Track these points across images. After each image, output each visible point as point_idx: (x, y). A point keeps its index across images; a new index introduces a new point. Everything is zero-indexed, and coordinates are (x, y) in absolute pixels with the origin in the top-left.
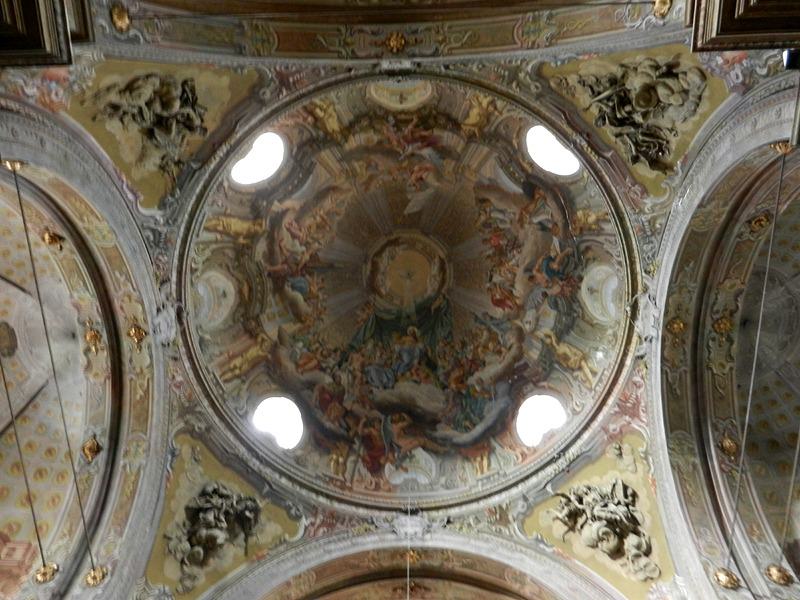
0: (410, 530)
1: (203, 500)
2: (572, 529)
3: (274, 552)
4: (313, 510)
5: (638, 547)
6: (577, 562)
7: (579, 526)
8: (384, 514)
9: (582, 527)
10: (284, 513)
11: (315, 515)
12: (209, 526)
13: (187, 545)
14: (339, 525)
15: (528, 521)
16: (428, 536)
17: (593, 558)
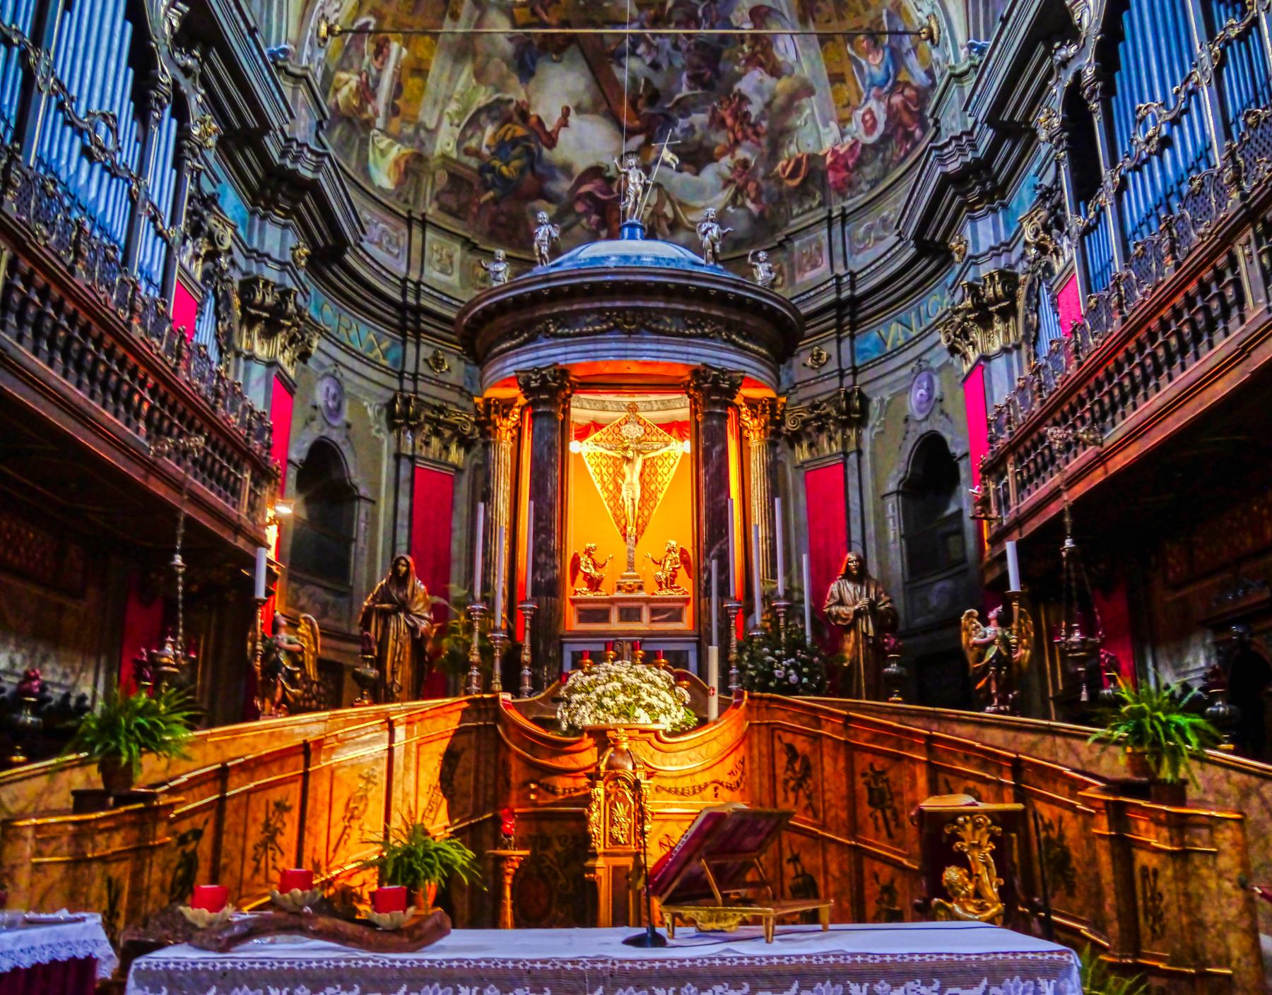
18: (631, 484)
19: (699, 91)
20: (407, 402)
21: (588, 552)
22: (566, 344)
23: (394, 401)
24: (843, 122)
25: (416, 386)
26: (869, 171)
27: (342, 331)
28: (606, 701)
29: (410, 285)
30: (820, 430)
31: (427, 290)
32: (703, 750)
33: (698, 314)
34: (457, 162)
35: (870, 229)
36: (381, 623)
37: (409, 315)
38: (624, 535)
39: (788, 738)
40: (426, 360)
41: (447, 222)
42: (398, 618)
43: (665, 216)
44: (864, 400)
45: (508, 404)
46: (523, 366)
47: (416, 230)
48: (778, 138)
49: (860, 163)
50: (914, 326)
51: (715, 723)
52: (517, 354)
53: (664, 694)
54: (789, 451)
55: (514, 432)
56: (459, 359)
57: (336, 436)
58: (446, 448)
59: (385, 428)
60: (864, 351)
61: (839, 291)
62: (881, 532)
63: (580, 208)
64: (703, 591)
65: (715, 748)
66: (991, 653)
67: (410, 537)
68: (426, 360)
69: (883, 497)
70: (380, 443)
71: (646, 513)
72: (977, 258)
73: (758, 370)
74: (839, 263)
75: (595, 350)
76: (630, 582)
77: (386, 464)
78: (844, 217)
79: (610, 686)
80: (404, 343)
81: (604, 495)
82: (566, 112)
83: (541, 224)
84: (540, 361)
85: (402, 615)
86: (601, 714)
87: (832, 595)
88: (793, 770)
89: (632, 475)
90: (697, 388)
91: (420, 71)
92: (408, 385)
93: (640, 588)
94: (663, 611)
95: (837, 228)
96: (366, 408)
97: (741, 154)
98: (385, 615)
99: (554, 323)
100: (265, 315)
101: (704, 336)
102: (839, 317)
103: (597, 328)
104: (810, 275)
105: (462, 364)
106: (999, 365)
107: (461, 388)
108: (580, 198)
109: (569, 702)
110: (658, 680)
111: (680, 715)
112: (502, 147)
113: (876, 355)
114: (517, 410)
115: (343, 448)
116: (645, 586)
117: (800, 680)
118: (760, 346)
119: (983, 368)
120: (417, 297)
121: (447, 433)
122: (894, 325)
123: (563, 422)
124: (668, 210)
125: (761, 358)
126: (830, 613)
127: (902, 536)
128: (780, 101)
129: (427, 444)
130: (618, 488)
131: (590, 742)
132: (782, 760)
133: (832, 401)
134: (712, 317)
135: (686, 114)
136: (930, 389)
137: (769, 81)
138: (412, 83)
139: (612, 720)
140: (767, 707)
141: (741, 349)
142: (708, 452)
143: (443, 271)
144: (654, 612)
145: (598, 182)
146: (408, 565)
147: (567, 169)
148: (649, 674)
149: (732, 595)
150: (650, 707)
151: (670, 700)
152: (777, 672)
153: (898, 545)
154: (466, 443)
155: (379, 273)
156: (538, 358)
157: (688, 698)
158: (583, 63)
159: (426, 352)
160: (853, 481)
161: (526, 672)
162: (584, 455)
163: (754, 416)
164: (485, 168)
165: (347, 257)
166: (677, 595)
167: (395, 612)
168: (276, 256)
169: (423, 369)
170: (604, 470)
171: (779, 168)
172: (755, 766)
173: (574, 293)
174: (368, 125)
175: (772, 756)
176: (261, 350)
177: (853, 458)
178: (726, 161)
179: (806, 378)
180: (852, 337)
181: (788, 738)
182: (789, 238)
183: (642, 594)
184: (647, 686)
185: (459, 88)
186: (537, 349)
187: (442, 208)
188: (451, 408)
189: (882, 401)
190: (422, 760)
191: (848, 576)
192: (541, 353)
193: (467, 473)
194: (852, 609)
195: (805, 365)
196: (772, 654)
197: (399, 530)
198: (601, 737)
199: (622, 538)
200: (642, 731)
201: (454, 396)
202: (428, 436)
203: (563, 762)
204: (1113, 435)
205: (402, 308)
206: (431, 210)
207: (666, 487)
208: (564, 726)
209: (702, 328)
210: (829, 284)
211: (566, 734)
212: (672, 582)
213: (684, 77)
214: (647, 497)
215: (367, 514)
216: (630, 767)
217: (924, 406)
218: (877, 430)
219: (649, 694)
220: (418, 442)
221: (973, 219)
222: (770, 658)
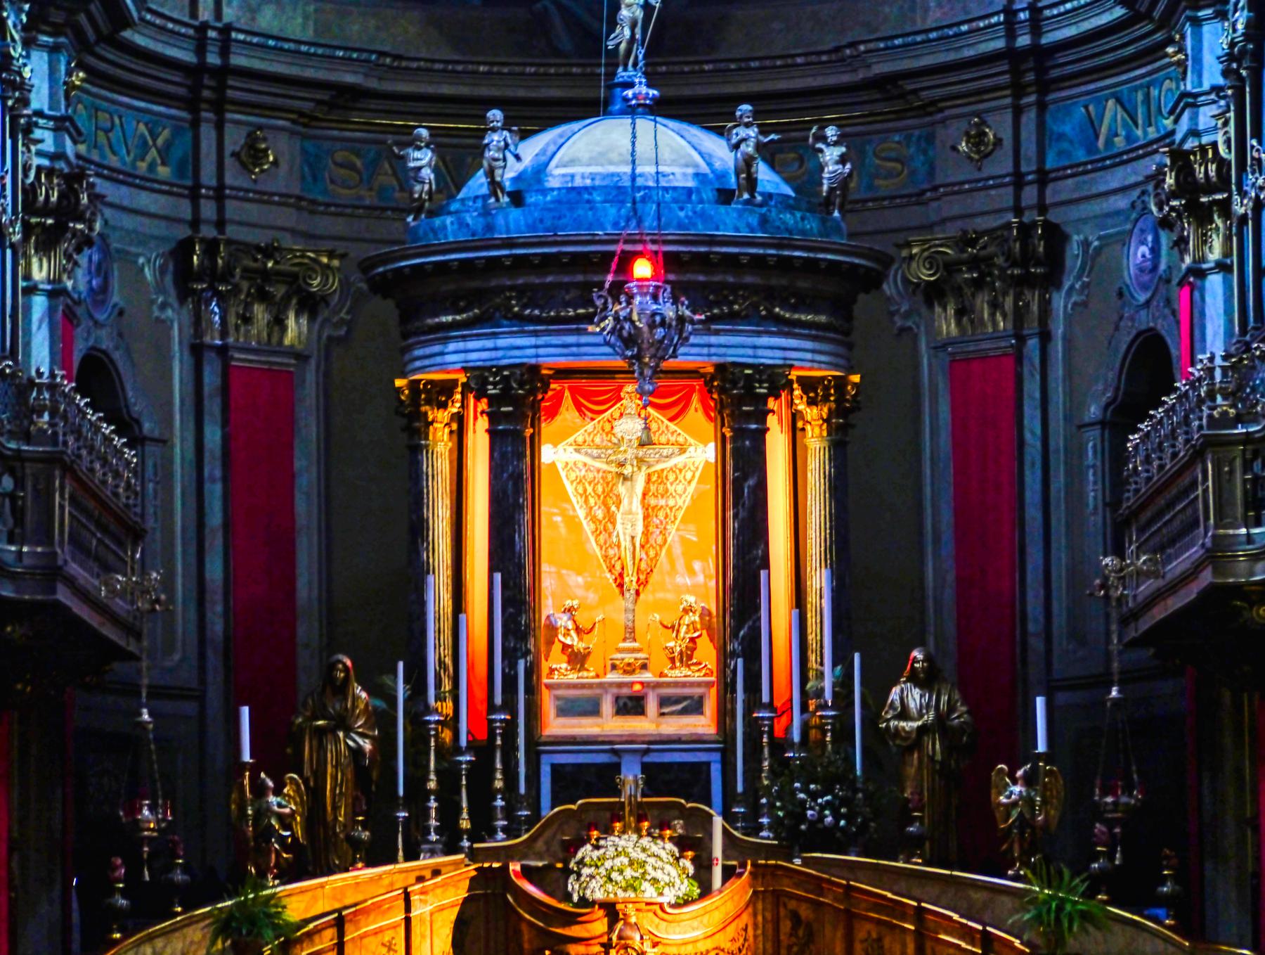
18: (630, 512)
20: (211, 248)
21: (569, 610)
22: (536, 334)
23: (182, 250)
25: (221, 210)
27: (102, 138)
28: (614, 875)
29: (212, 34)
30: (978, 284)
31: (241, 37)
32: (706, 917)
33: (723, 285)
36: (315, 743)
37: (207, 81)
38: (621, 586)
39: (792, 904)
40: (235, 155)
42: (337, 739)
44: (1056, 237)
45: (446, 389)
46: (474, 356)
50: (1140, 122)
51: (720, 891)
52: (464, 338)
53: (668, 868)
54: (924, 310)
55: (455, 426)
56: (293, 133)
58: (279, 323)
59: (173, 299)
60: (1061, 137)
61: (1011, 35)
64: (727, 687)
65: (717, 917)
66: (1015, 814)
68: (235, 155)
69: (1080, 427)
70: (164, 325)
71: (652, 553)
72: (1196, 96)
73: (813, 351)
75: (579, 345)
76: (629, 658)
79: (617, 862)
80: (195, 124)
81: (588, 527)
83: (494, 130)
84: (500, 353)
85: (341, 734)
86: (610, 887)
87: (892, 706)
88: (797, 937)
89: (631, 498)
90: (722, 390)
92: (208, 210)
93: (644, 667)
94: (678, 700)
96: (142, 270)
99: (518, 299)
100: (50, 221)
101: (733, 317)
102: (1016, 73)
103: (581, 311)
105: (297, 143)
106: (1215, 282)
107: (300, 198)
109: (579, 875)
110: (663, 854)
111: (687, 887)
113: (1081, 155)
114: (458, 397)
115: (117, 355)
116: (651, 666)
117: (837, 822)
118: (817, 312)
119: (1192, 286)
120: (225, 52)
121: (279, 291)
122: (1111, 103)
123: (532, 436)
125: (815, 332)
126: (888, 727)
127: (1105, 504)
129: (247, 320)
130: (611, 519)
131: (601, 913)
132: (786, 926)
134: (745, 287)
136: (1155, 250)
139: (621, 894)
140: (774, 875)
141: (787, 327)
142: (738, 485)
144: (664, 701)
146: (346, 669)
148: (654, 848)
149: (765, 698)
150: (655, 881)
151: (674, 872)
152: (809, 813)
153: (1099, 519)
154: (310, 305)
155: (163, 29)
156: (496, 349)
157: (691, 870)
159: (235, 139)
160: (1032, 388)
161: (499, 803)
162: (560, 466)
163: (812, 402)
165: (127, 34)
166: (697, 677)
167: (332, 730)
168: (47, 111)
170: (590, 489)
172: (759, 932)
175: (776, 922)
176: (40, 272)
177: (1033, 344)
179: (961, 178)
180: (1042, 107)
181: (792, 904)
183: (647, 676)
184: (651, 860)
186: (494, 335)
188: (287, 241)
189: (1086, 244)
190: (434, 928)
191: (914, 679)
192: (501, 342)
193: (313, 362)
194: (915, 724)
195: (954, 148)
196: (805, 789)
197: (207, 486)
198: (611, 911)
199: (617, 591)
200: (648, 904)
201: (287, 217)
202: (248, 306)
203: (575, 931)
204: (1178, 565)
205: (195, 72)
207: (680, 515)
208: (575, 898)
209: (731, 304)
210: (994, 20)
211: (576, 905)
212: (690, 658)
215: (155, 466)
216: (638, 937)
217: (1146, 278)
218: (1074, 298)
219: (655, 869)
220: (232, 320)
221: (1197, 23)
222: (802, 796)
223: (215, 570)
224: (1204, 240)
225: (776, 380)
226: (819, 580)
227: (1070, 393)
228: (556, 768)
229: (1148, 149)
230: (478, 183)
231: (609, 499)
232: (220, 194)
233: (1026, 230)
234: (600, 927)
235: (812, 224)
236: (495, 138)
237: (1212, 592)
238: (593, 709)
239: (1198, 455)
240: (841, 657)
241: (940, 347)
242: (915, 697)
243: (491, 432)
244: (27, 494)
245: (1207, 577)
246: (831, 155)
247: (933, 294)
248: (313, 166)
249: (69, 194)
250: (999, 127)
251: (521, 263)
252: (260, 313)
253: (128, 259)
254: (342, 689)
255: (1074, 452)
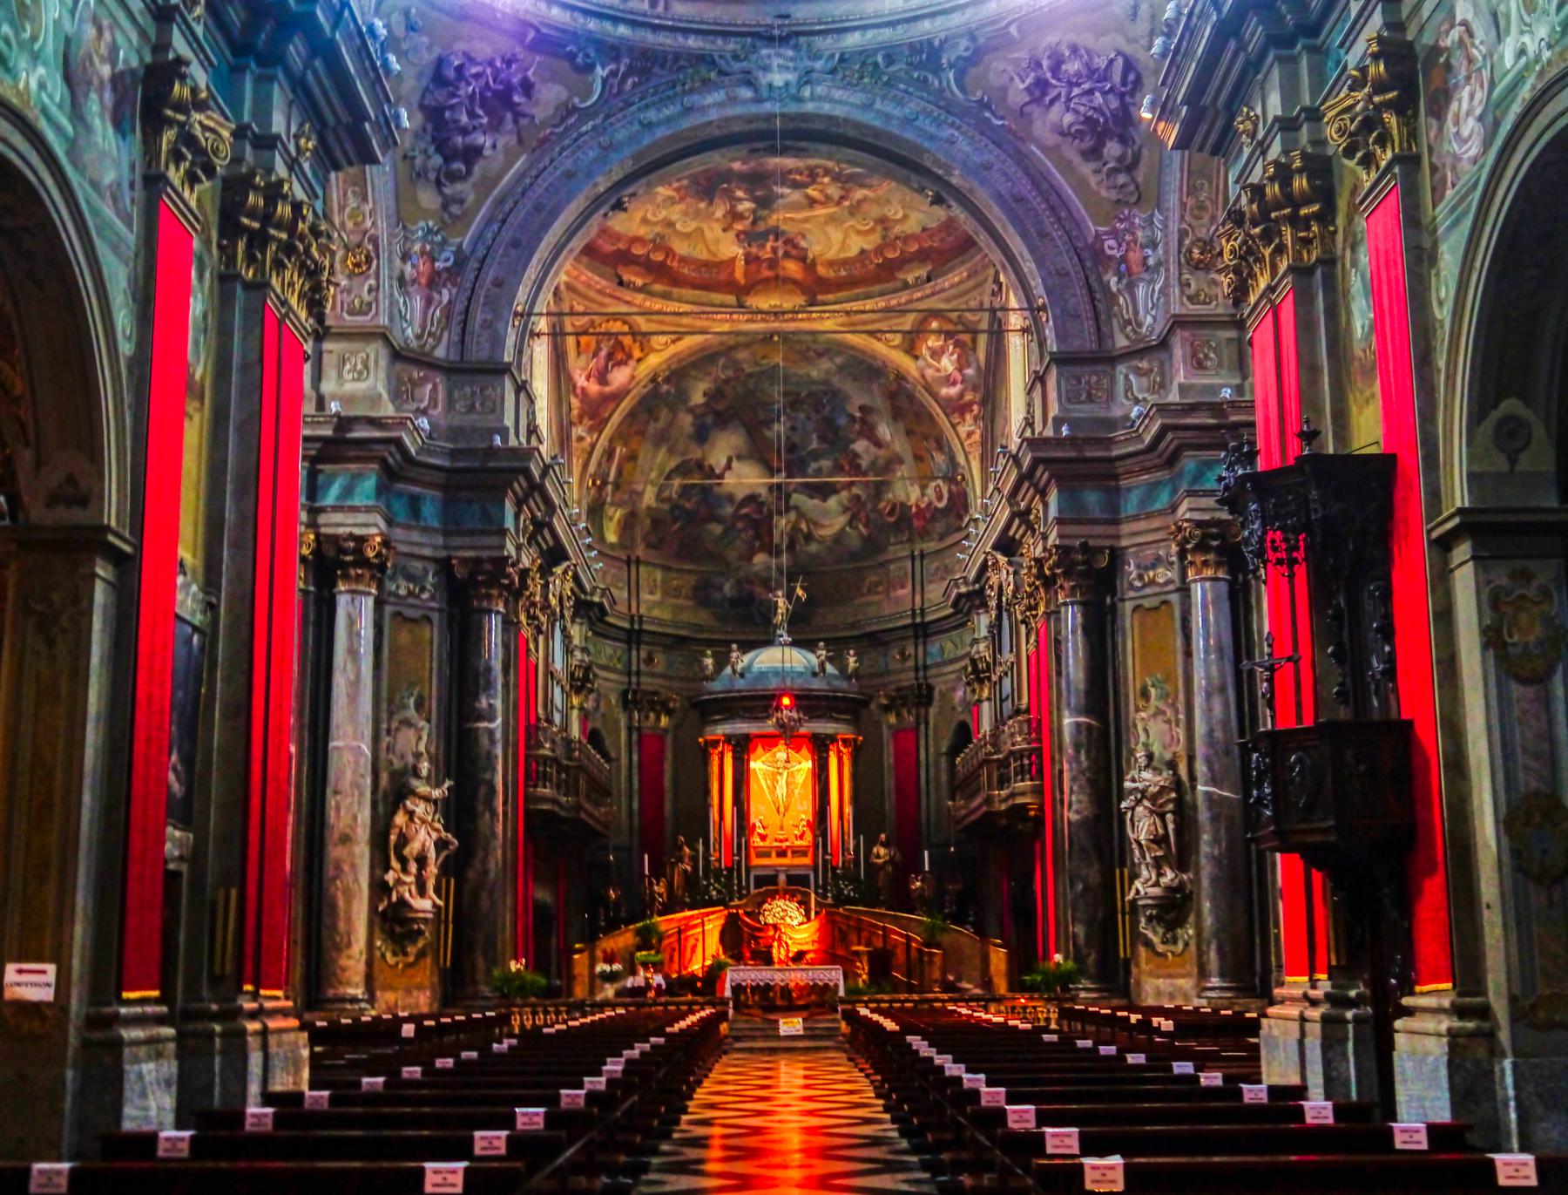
0: (778, 79)
1: (444, 92)
2: (1036, 101)
3: (560, 129)
4: (612, 51)
5: (1120, 159)
6: (1033, 148)
7: (1048, 99)
8: (732, 45)
9: (1052, 102)
10: (566, 65)
11: (617, 59)
12: (465, 132)
13: (437, 160)
14: (657, 70)
15: (973, 71)
16: (807, 92)
17: (1057, 147)
19: (825, 446)
23: (624, 694)
24: (923, 488)
26: (939, 527)
30: (903, 705)
34: (656, 509)
35: (937, 569)
41: (652, 556)
43: (801, 530)
44: (930, 688)
47: (633, 568)
48: (879, 489)
49: (933, 519)
57: (598, 725)
58: (658, 719)
62: (937, 778)
63: (740, 525)
64: (816, 846)
67: (640, 781)
70: (617, 722)
74: (918, 588)
77: (623, 735)
78: (922, 556)
80: (630, 650)
82: (730, 460)
89: (782, 781)
91: (632, 457)
92: (634, 679)
95: (918, 563)
97: (855, 490)
98: (673, 865)
104: (901, 592)
108: (741, 518)
111: (801, 919)
112: (685, 491)
124: (803, 526)
128: (881, 462)
129: (647, 717)
133: (910, 688)
135: (816, 459)
137: (873, 449)
138: (628, 467)
141: (837, 720)
143: (651, 593)
145: (753, 506)
147: (730, 498)
154: (669, 712)
158: (742, 431)
159: (643, 654)
160: (922, 742)
164: (675, 506)
169: (643, 667)
171: (882, 505)
173: (752, 698)
174: (603, 504)
176: (575, 701)
178: (844, 494)
182: (890, 561)
185: (658, 460)
187: (650, 546)
191: (883, 845)
198: (776, 927)
201: (661, 681)
204: (975, 804)
205: (630, 632)
206: (640, 551)
213: (814, 436)
214: (790, 794)
223: (636, 805)
224: (982, 690)
225: (833, 739)
226: (848, 809)
227: (936, 741)
228: (756, 878)
229: (962, 658)
230: (728, 670)
231: (774, 781)
232: (638, 673)
233: (920, 686)
234: (771, 933)
235: (844, 685)
236: (734, 655)
237: (987, 814)
238: (768, 855)
239: (981, 765)
240: (856, 837)
241: (890, 727)
242: (882, 851)
243: (734, 758)
244: (571, 781)
245: (984, 809)
246: (852, 660)
247: (886, 709)
248: (670, 664)
249: (586, 675)
250: (910, 650)
251: (743, 698)
252: (652, 715)
253: (606, 696)
254: (680, 848)
255: (937, 764)
